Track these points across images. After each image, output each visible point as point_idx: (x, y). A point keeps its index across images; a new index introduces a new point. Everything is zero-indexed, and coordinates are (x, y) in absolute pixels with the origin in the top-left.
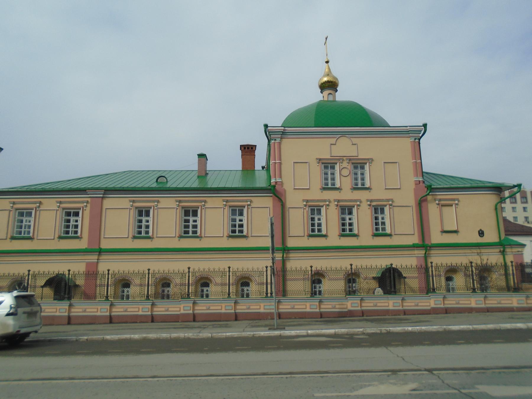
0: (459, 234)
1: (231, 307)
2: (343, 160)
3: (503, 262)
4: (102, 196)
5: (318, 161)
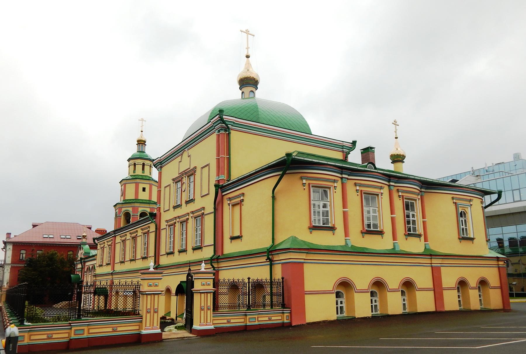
0: (243, 238)
1: (259, 320)
2: (183, 174)
3: (269, 278)
4: (114, 235)
5: (173, 181)
